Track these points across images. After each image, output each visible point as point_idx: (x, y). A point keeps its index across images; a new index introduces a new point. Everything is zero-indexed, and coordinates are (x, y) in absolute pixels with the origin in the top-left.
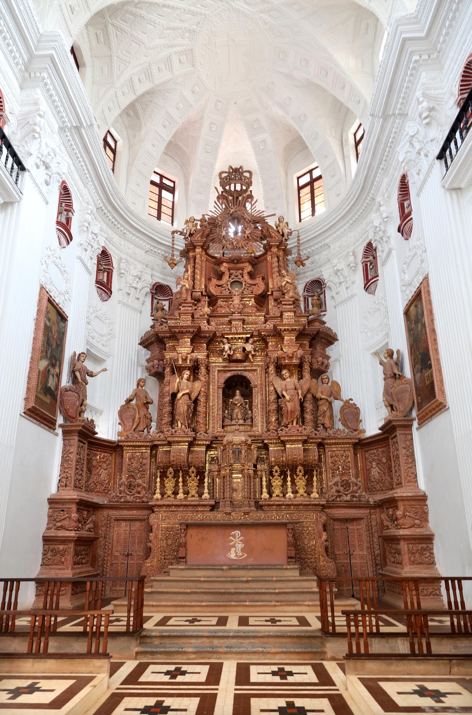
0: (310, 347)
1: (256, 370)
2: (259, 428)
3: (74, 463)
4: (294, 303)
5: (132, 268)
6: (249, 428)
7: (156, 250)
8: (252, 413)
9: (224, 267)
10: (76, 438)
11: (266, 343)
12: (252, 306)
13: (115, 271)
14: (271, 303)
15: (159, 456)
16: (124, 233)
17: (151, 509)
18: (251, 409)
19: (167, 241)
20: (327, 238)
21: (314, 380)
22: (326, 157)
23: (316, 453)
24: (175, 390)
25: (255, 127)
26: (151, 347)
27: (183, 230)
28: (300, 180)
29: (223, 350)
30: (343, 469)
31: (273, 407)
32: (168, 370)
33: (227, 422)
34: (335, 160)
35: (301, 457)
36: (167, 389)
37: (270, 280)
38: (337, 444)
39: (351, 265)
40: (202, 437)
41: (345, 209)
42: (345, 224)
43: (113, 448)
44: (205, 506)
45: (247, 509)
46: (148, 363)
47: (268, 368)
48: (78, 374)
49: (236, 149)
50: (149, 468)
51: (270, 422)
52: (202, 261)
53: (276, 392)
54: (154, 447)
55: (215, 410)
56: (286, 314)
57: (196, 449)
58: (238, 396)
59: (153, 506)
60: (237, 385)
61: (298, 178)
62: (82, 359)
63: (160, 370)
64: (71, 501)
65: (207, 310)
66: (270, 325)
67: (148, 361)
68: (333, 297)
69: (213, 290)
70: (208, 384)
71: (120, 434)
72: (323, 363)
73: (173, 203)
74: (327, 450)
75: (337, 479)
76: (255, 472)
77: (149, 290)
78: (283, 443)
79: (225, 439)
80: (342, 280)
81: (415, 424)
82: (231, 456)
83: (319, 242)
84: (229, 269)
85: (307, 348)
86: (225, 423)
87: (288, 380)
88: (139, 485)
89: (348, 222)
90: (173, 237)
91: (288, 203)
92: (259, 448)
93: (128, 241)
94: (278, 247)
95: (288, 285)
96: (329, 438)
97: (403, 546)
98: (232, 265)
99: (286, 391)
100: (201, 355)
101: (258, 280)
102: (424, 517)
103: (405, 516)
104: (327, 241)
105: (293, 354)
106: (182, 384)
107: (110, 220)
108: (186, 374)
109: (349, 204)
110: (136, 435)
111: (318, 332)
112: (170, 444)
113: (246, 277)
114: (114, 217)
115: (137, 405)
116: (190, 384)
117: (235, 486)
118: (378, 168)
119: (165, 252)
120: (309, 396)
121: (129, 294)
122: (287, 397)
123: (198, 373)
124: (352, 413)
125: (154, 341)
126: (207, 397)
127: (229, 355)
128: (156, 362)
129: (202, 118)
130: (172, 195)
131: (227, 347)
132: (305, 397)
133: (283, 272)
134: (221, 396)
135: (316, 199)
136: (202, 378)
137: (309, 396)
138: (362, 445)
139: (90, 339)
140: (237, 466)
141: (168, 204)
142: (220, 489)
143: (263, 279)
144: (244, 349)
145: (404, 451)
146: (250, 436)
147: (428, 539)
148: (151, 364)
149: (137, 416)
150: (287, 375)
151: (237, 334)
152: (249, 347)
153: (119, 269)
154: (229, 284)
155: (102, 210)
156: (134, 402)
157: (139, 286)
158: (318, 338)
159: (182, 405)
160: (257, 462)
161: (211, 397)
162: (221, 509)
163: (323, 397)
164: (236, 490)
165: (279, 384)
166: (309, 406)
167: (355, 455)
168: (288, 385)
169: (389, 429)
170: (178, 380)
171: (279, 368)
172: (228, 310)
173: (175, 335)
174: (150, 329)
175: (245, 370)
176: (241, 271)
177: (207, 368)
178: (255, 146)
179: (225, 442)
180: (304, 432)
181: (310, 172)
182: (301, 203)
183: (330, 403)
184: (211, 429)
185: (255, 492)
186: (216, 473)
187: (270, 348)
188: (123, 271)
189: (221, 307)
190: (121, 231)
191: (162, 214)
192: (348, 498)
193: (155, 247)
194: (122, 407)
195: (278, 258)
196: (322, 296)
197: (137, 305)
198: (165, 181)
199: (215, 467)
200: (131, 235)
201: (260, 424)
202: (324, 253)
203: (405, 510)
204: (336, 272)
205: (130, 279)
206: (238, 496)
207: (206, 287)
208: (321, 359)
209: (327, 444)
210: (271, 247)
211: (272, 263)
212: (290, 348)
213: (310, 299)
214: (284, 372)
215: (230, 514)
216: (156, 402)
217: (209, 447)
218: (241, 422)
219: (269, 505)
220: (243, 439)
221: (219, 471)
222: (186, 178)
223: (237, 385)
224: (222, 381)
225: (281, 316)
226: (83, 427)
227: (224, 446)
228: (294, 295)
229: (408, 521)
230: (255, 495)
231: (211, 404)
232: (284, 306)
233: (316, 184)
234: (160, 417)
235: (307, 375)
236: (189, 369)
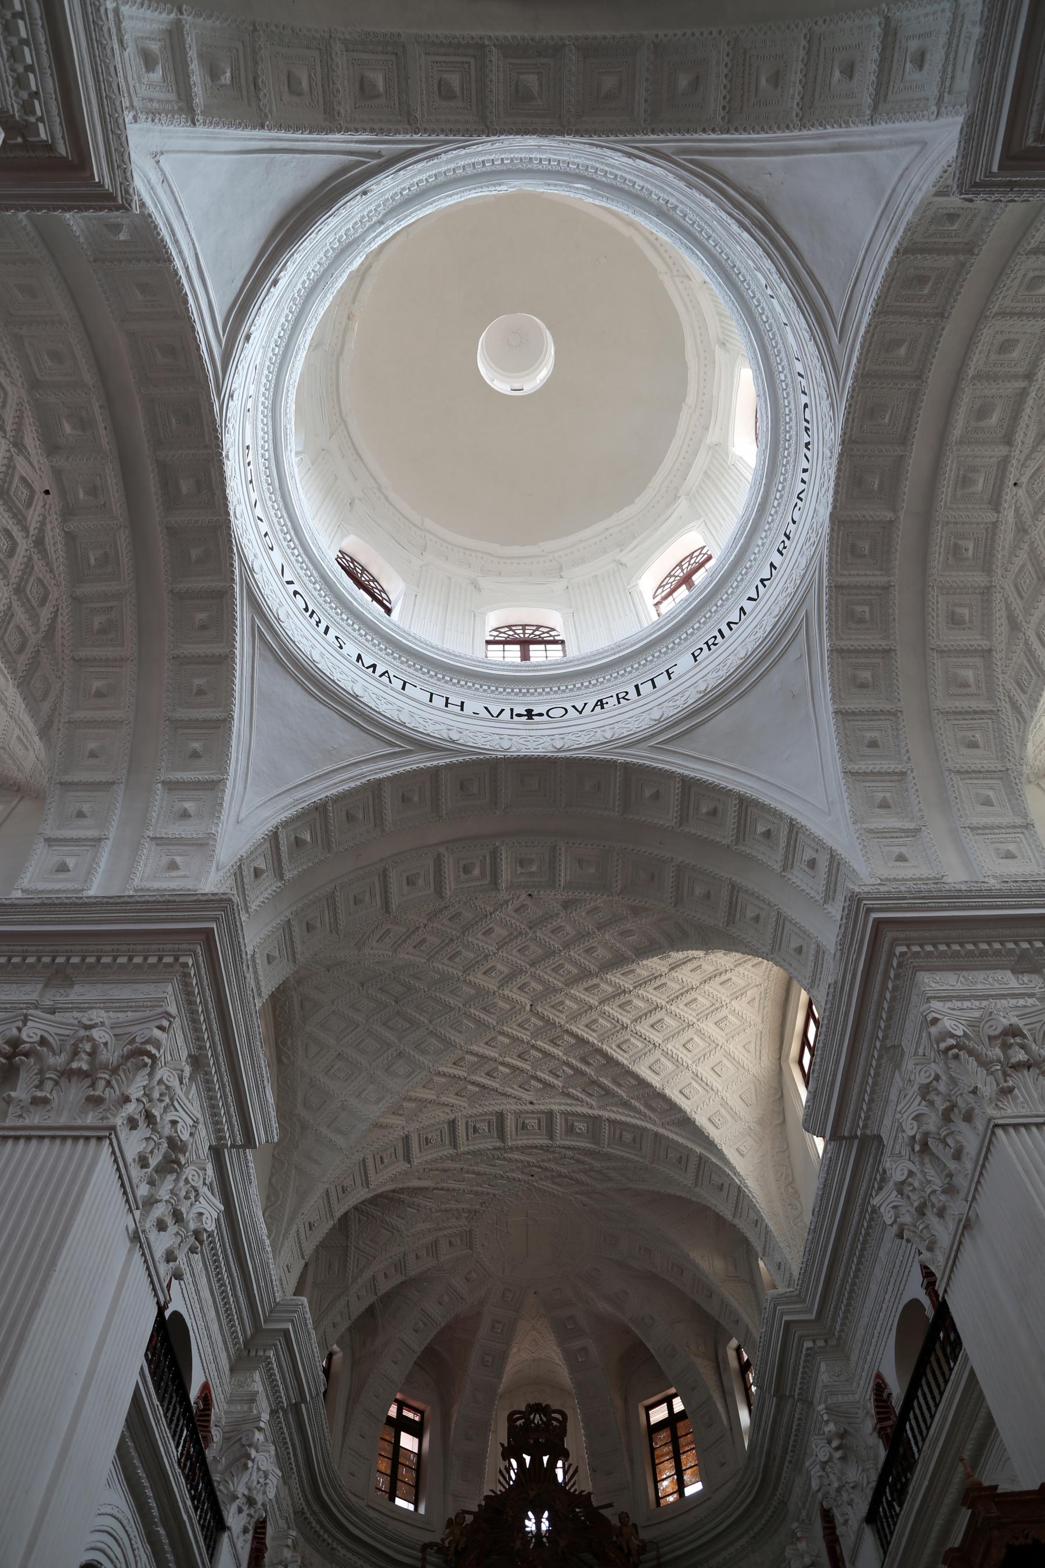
16: (333, 1549)
19: (408, 1556)
22: (694, 1389)
25: (569, 1327)
27: (443, 1540)
34: (710, 1397)
41: (738, 1508)
73: (419, 1455)
90: (424, 1559)
91: (632, 1461)
107: (312, 1528)
109: (743, 1501)
114: (319, 1522)
118: (783, 1458)
130: (416, 1440)
135: (683, 1457)
141: (409, 1460)
155: (303, 1513)
178: (570, 1358)
181: (669, 1400)
182: (657, 1461)
190: (328, 1544)
191: (399, 1483)
198: (407, 1414)
200: (343, 1551)
233: (681, 1427)
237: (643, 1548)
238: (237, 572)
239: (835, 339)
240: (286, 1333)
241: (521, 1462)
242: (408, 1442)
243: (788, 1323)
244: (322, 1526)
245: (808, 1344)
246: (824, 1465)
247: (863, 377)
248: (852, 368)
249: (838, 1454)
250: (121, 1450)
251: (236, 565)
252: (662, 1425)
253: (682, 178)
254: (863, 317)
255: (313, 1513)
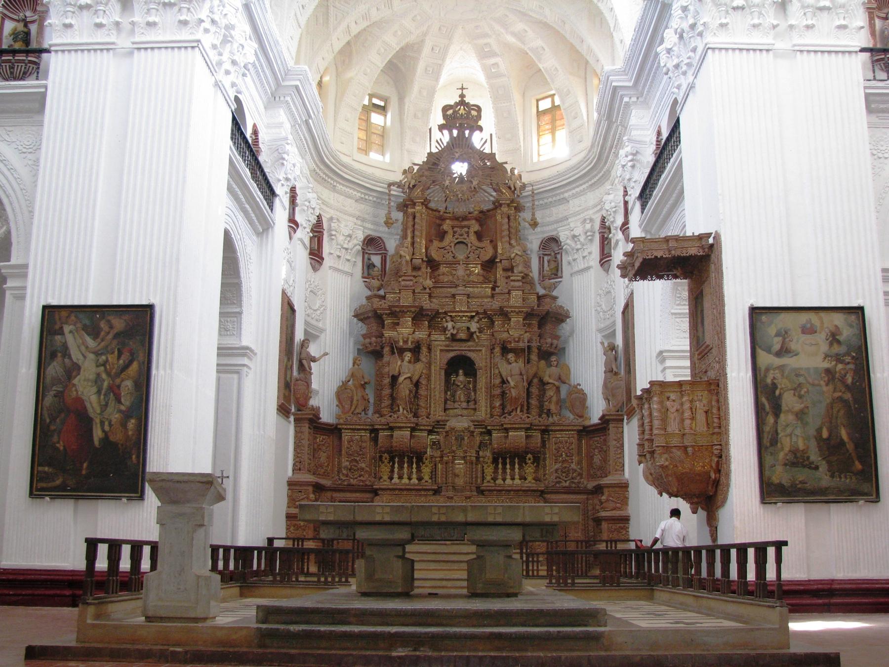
0: (539, 328)
1: (480, 350)
2: (482, 413)
3: (307, 449)
4: (523, 278)
5: (342, 226)
6: (472, 412)
7: (367, 197)
8: (475, 394)
9: (446, 226)
10: (307, 425)
11: (493, 322)
12: (478, 274)
13: (325, 232)
14: (500, 273)
15: (380, 440)
17: (375, 492)
18: (475, 390)
20: (567, 191)
21: (543, 362)
23: (539, 440)
24: (396, 373)
26: (367, 321)
28: (540, 103)
29: (445, 329)
30: (567, 456)
31: (498, 391)
32: (387, 350)
33: (450, 404)
35: (524, 444)
36: (386, 370)
37: (499, 244)
38: (562, 430)
39: (589, 234)
40: (424, 423)
42: (585, 183)
43: (333, 431)
44: (429, 490)
45: (468, 493)
46: (365, 339)
47: (494, 348)
48: (304, 362)
49: (461, 72)
50: (369, 450)
51: (494, 408)
52: (422, 219)
53: (501, 375)
54: (374, 431)
55: (437, 393)
56: (514, 293)
57: (417, 434)
58: (461, 378)
59: (377, 489)
60: (461, 364)
61: (538, 101)
62: (306, 345)
63: (378, 348)
64: (307, 484)
65: (429, 283)
66: (496, 304)
67: (364, 336)
68: (569, 263)
69: (435, 255)
70: (429, 365)
71: (338, 417)
72: (552, 344)
74: (551, 437)
75: (558, 466)
76: (478, 458)
77: (360, 248)
78: (507, 430)
79: (448, 424)
80: (579, 246)
81: (625, 417)
82: (453, 442)
83: (558, 194)
84: (453, 227)
85: (536, 329)
86: (448, 406)
87: (514, 364)
88: (363, 469)
89: (587, 182)
92: (481, 433)
93: (338, 193)
94: (508, 205)
95: (517, 257)
96: (553, 424)
97: (604, 525)
98: (456, 223)
99: (511, 376)
100: (421, 335)
101: (486, 243)
102: (625, 501)
103: (607, 500)
104: (566, 195)
105: (519, 338)
106: (405, 368)
108: (408, 356)
110: (355, 418)
111: (548, 313)
112: (391, 429)
113: (473, 237)
114: (324, 173)
115: (354, 385)
116: (411, 366)
117: (457, 471)
119: (377, 198)
120: (535, 381)
121: (339, 257)
122: (512, 384)
123: (419, 352)
124: (579, 399)
125: (374, 317)
126: (429, 380)
127: (452, 334)
128: (374, 339)
129: (423, 41)
131: (450, 325)
132: (530, 384)
133: (513, 242)
134: (443, 377)
136: (424, 360)
137: (535, 381)
138: (587, 432)
139: (309, 319)
140: (460, 453)
142: (442, 474)
143: (491, 241)
144: (468, 328)
145: (615, 442)
146: (473, 421)
147: (626, 519)
148: (368, 340)
149: (355, 398)
150: (513, 359)
151: (462, 312)
152: (474, 327)
153: (330, 230)
154: (452, 245)
155: (315, 170)
156: (350, 383)
157: (350, 246)
158: (548, 318)
159: (404, 389)
160: (479, 448)
161: (433, 379)
162: (443, 493)
163: (551, 381)
164: (458, 476)
165: (504, 368)
166: (534, 390)
167: (580, 440)
168: (512, 369)
169: (605, 420)
170: (399, 363)
171: (505, 350)
172: (451, 278)
173: (396, 313)
174: (364, 302)
175: (469, 350)
176: (466, 229)
177: (429, 349)
178: (486, 70)
179: (447, 428)
180: (527, 420)
181: (553, 96)
183: (558, 388)
184: (432, 412)
185: (477, 477)
186: (438, 459)
187: (496, 328)
188: (334, 233)
189: (443, 274)
192: (567, 484)
193: (365, 194)
194: (340, 387)
195: (509, 218)
196: (559, 256)
197: (347, 267)
198: (376, 101)
199: (438, 454)
201: (484, 409)
202: (562, 208)
203: (609, 496)
204: (574, 237)
205: (341, 238)
206: (460, 482)
207: (427, 249)
208: (549, 340)
209: (552, 431)
210: (501, 205)
211: (502, 225)
212: (515, 331)
213: (546, 258)
214: (511, 356)
215: (452, 498)
216: (373, 382)
217: (430, 432)
218: (464, 405)
219: (489, 490)
220: (466, 425)
221: (442, 457)
222: (401, 99)
223: (461, 364)
224: (445, 361)
225: (509, 293)
226: (314, 415)
227: (447, 432)
228: (525, 270)
229: (611, 505)
230: (476, 480)
231: (433, 386)
232: (512, 283)
234: (379, 398)
235: (534, 357)
236: (410, 350)
237: (524, 186)
240: (297, 87)
241: (451, 134)
242: (376, 119)
243: (615, 88)
244: (327, 175)
245: (626, 99)
246: (623, 166)
249: (630, 164)
250: (230, 189)
252: (545, 112)
255: (320, 169)
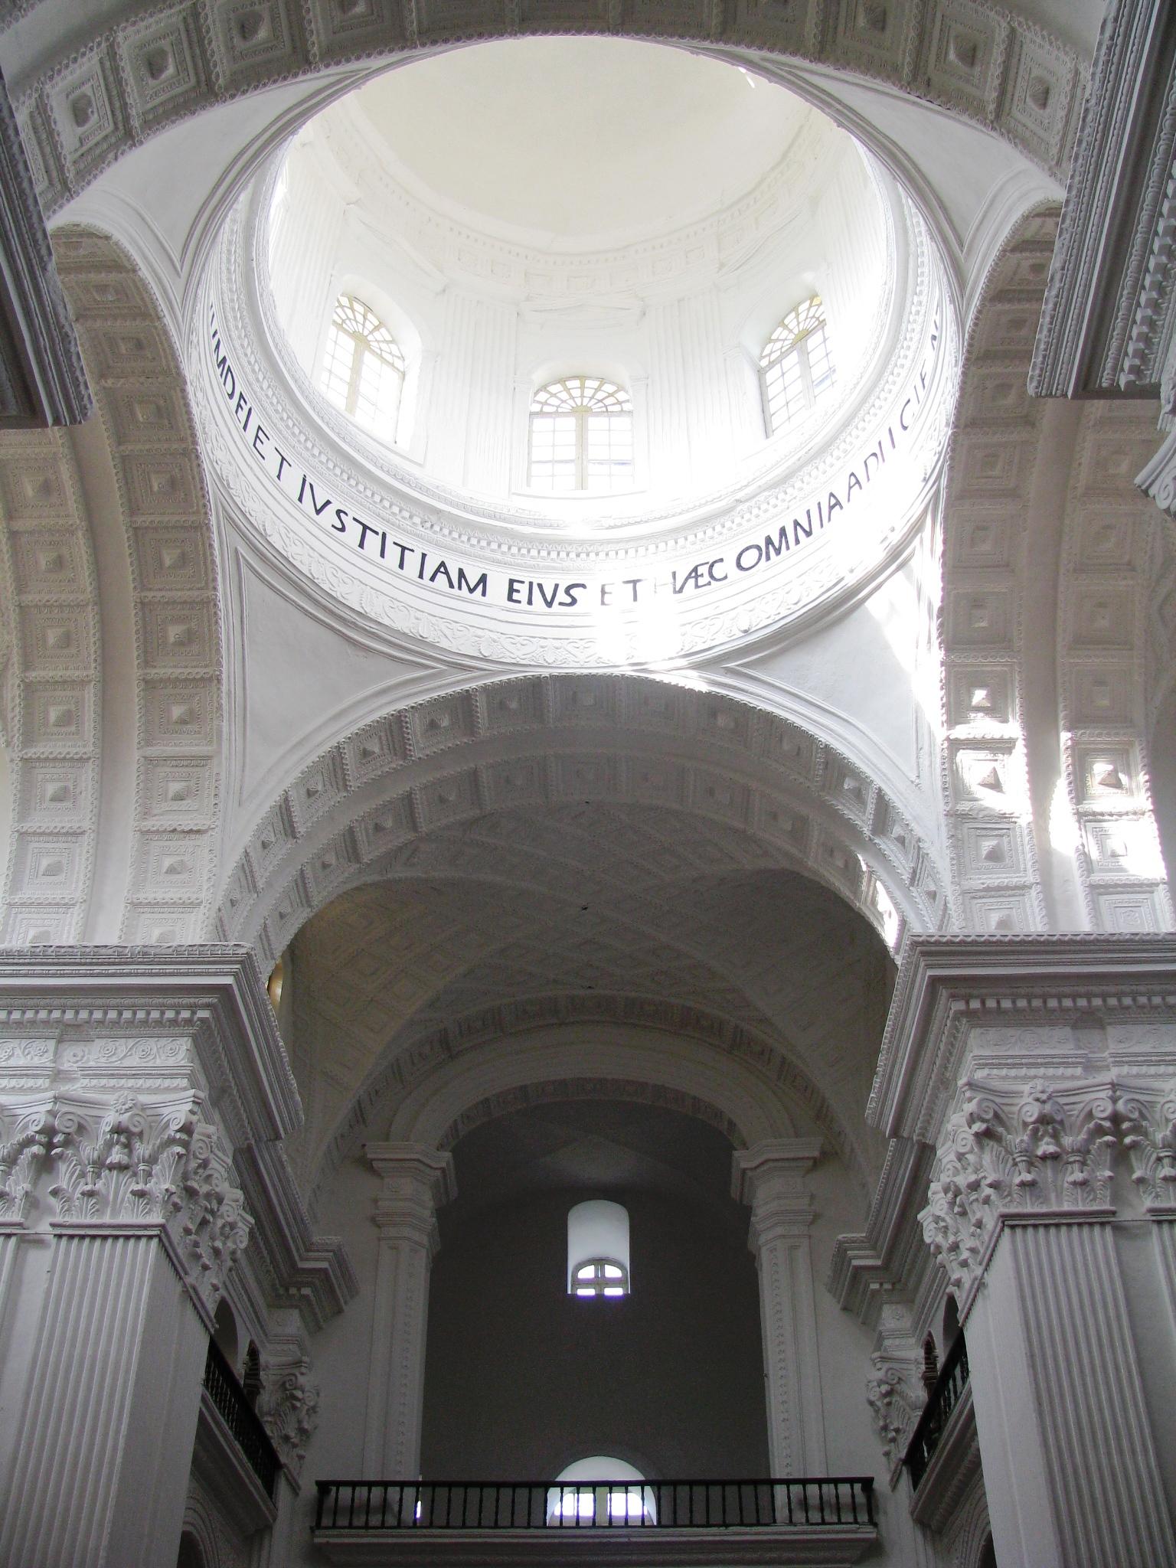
238: (971, 316)
239: (243, 550)
247: (201, 528)
248: (215, 536)
251: (969, 323)
253: (432, 646)
254: (224, 592)
